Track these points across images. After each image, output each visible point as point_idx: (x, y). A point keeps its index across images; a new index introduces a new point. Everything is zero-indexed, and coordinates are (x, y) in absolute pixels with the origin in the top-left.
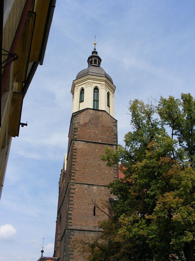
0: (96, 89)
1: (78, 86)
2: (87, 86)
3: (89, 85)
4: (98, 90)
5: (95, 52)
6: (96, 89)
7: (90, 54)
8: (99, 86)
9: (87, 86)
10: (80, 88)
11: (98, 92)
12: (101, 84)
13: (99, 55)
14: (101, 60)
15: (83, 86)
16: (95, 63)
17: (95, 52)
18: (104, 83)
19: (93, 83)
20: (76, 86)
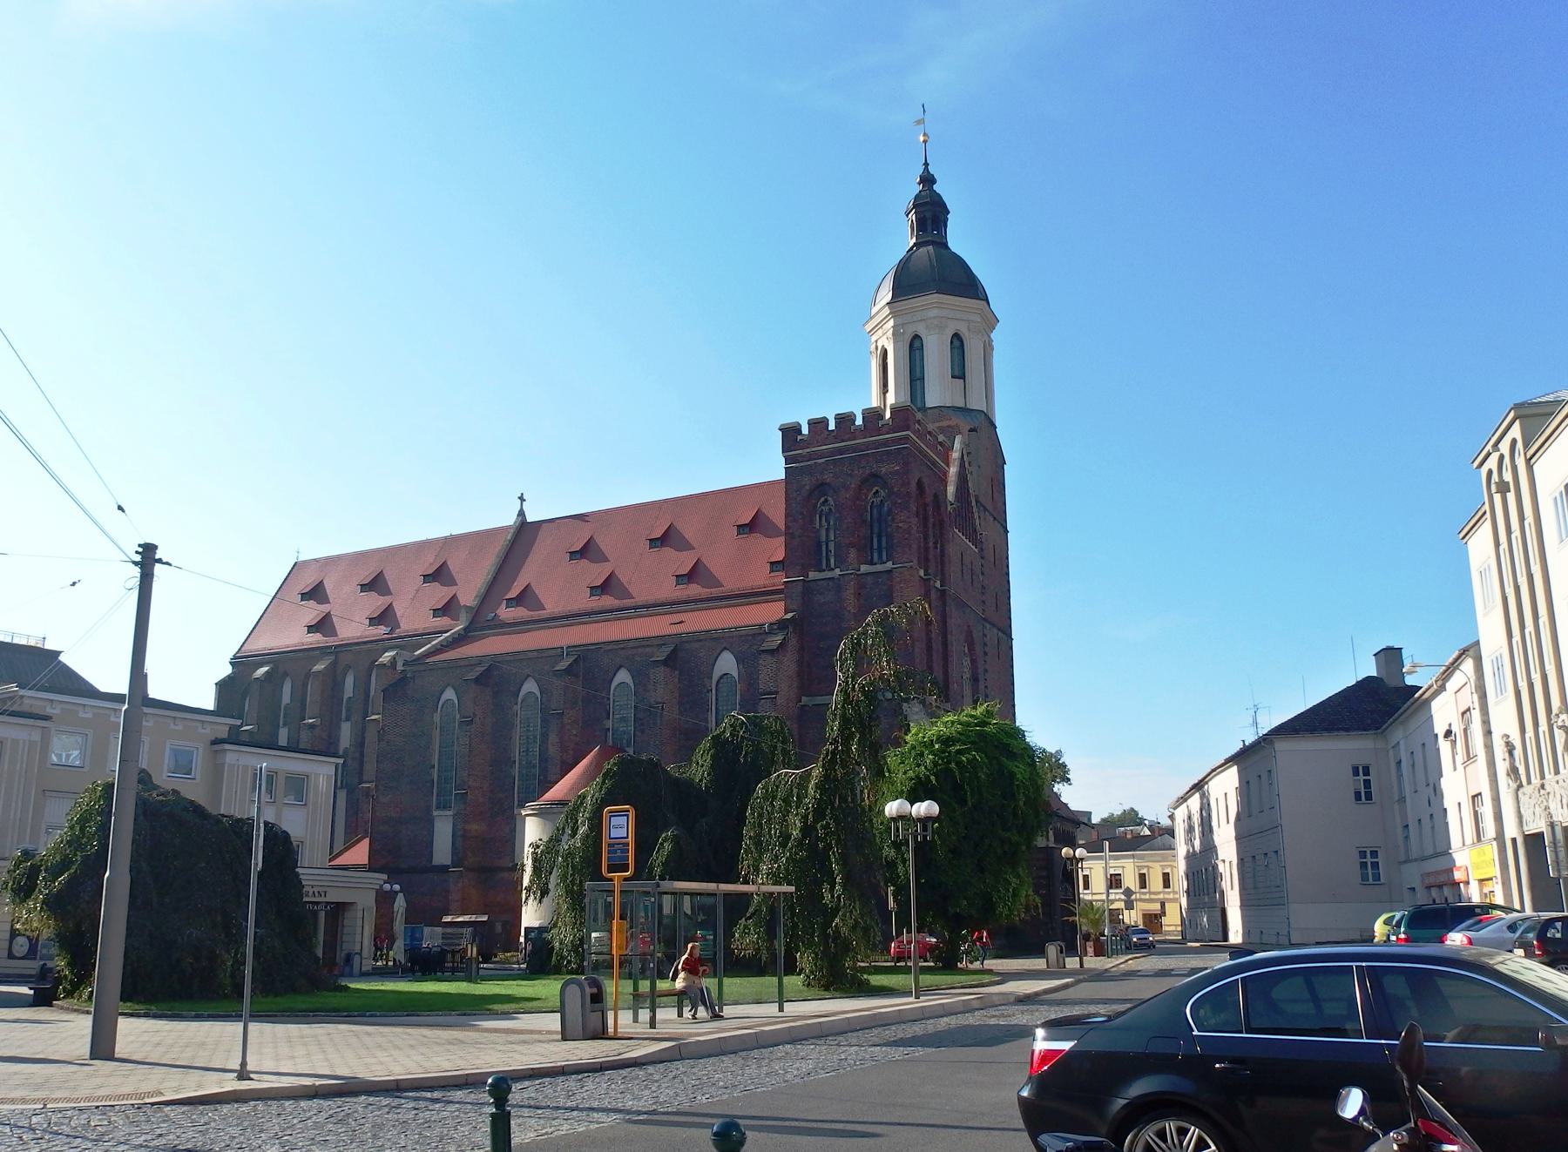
5: (927, 180)
17: (927, 180)
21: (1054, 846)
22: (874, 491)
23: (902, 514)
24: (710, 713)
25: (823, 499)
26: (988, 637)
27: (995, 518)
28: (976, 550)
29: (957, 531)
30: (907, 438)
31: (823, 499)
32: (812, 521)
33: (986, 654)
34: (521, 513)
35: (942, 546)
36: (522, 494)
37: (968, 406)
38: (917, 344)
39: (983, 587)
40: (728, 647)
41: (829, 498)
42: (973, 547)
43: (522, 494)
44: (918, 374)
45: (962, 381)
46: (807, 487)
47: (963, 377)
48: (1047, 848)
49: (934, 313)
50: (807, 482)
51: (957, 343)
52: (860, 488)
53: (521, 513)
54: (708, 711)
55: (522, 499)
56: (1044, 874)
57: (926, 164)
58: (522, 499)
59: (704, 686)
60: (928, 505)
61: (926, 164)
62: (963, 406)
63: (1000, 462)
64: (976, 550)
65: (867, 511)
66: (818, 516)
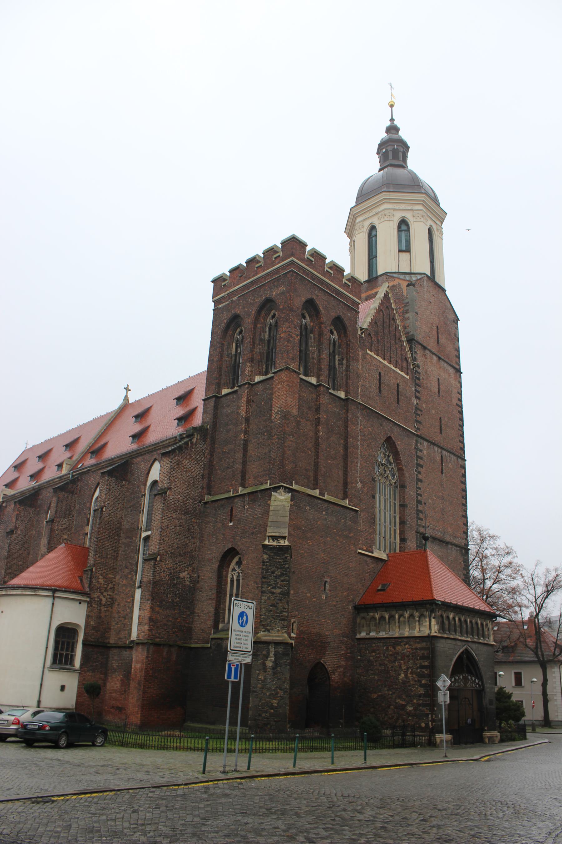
0: (403, 226)
1: (363, 221)
2: (382, 220)
3: (386, 218)
4: (407, 225)
5: (392, 129)
6: (403, 226)
7: (383, 135)
8: (409, 216)
9: (382, 220)
10: (367, 224)
11: (408, 230)
12: (412, 210)
13: (403, 134)
14: (408, 148)
15: (375, 221)
16: (395, 156)
17: (392, 129)
18: (420, 207)
19: (395, 209)
20: (359, 222)
21: (435, 634)
22: (272, 314)
23: (284, 326)
24: (141, 515)
25: (239, 330)
26: (425, 452)
27: (440, 358)
28: (408, 377)
29: (373, 354)
30: (292, 263)
31: (239, 330)
32: (229, 348)
33: (419, 465)
34: (126, 398)
35: (348, 362)
36: (128, 386)
37: (412, 272)
38: (373, 233)
39: (417, 408)
40: (157, 458)
41: (243, 328)
42: (403, 374)
43: (128, 386)
44: (374, 254)
45: (408, 254)
46: (225, 321)
47: (408, 251)
48: (430, 638)
49: (386, 206)
50: (226, 317)
51: (404, 227)
52: (259, 312)
53: (126, 398)
54: (140, 513)
55: (127, 389)
56: (426, 663)
57: (392, 120)
58: (127, 389)
59: (141, 492)
60: (323, 323)
61: (392, 120)
62: (409, 271)
63: (452, 317)
64: (408, 377)
65: (265, 332)
66: (234, 345)
